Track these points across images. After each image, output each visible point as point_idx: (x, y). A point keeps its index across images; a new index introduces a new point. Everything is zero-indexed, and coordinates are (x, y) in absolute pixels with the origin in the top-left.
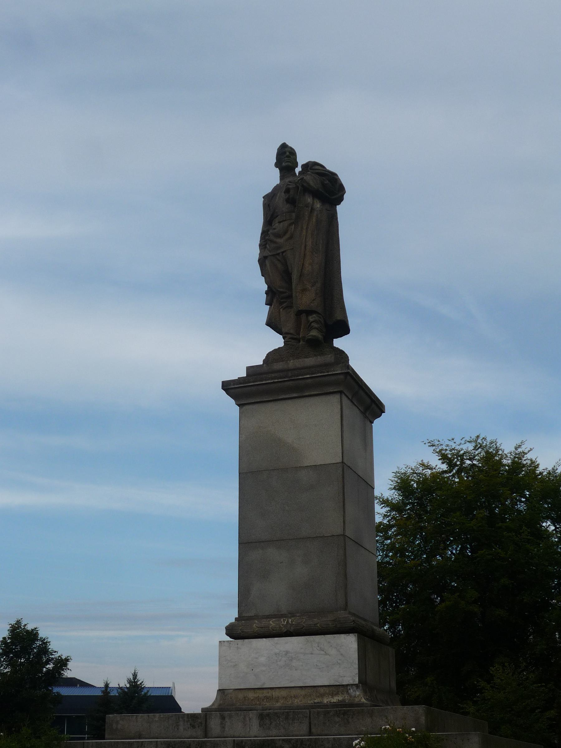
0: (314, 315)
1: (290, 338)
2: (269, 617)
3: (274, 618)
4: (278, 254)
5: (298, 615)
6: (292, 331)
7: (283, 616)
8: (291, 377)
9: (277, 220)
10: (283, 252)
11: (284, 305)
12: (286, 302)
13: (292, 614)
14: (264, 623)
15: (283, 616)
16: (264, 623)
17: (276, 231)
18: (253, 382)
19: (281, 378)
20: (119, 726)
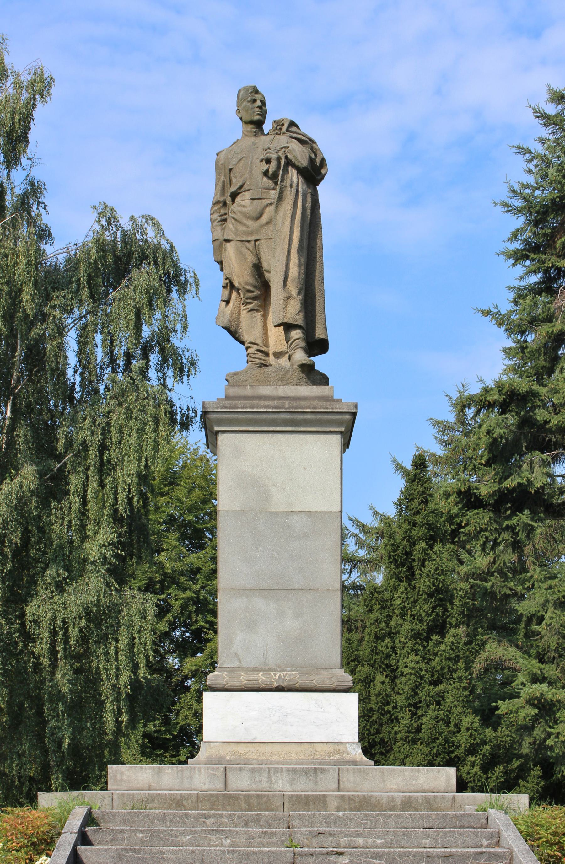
0: (299, 331)
1: (257, 350)
2: (261, 669)
3: (264, 671)
4: (248, 241)
5: (288, 669)
6: (258, 341)
7: (271, 669)
8: (289, 408)
9: (247, 195)
10: (256, 241)
11: (250, 306)
12: (252, 303)
13: (281, 669)
14: (252, 675)
15: (271, 669)
16: (252, 675)
17: (245, 209)
18: (242, 408)
19: (276, 408)
20: (125, 777)
